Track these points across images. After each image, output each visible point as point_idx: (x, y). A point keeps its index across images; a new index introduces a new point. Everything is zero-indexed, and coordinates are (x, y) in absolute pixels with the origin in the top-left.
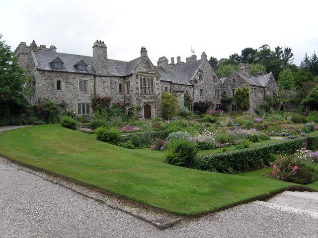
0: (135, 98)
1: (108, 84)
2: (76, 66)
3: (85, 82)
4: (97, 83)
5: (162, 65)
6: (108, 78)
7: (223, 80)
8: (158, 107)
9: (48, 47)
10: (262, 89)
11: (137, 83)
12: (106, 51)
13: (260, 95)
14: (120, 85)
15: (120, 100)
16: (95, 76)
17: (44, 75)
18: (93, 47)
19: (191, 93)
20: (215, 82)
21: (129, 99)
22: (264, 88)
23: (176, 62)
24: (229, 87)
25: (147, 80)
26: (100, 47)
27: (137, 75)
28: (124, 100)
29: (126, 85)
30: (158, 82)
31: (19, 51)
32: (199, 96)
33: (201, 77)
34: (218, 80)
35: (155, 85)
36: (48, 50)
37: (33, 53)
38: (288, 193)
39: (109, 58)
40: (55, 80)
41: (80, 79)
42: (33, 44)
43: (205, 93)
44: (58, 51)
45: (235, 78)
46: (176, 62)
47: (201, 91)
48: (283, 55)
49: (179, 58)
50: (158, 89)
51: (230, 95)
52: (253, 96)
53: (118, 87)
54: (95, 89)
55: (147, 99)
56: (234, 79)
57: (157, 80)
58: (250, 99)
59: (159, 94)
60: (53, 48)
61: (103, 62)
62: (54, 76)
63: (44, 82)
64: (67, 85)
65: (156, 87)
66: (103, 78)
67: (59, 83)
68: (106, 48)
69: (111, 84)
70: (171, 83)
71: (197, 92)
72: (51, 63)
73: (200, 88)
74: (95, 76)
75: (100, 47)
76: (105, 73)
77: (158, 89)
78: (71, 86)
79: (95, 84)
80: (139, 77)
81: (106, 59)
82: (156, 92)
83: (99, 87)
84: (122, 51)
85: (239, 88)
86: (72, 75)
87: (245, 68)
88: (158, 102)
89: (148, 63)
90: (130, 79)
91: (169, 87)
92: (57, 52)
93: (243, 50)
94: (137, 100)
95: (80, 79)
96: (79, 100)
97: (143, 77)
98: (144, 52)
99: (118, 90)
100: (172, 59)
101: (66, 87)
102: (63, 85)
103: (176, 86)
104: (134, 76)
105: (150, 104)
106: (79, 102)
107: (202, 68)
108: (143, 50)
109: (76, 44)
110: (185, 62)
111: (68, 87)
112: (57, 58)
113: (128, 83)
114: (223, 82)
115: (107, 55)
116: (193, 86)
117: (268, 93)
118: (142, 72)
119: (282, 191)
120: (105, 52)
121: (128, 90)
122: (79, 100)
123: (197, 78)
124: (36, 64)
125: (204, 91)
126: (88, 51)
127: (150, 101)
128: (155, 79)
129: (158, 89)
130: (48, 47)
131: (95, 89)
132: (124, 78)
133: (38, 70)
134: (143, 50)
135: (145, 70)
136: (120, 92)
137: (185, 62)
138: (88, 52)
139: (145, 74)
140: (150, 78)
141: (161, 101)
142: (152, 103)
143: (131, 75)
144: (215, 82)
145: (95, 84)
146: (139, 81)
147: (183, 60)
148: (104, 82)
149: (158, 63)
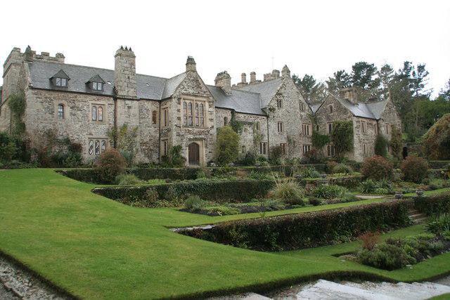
0: (175, 133)
1: (135, 111)
2: (88, 84)
3: (101, 106)
4: (118, 110)
5: (222, 84)
6: (135, 102)
7: (314, 109)
8: (209, 146)
9: (53, 55)
10: (375, 123)
11: (179, 111)
12: (134, 61)
13: (371, 132)
14: (154, 113)
15: (153, 134)
16: (115, 99)
17: (40, 96)
18: (116, 56)
19: (263, 126)
20: (302, 110)
21: (166, 135)
22: (377, 121)
23: (248, 80)
24: (324, 118)
25: (194, 106)
26: (125, 55)
27: (179, 99)
28: (160, 135)
29: (163, 112)
30: (211, 109)
31: (10, 62)
32: (277, 132)
33: (280, 103)
34: (307, 108)
35: (208, 114)
36: (54, 59)
37: (26, 64)
38: (323, 284)
39: (138, 71)
40: (56, 103)
41: (94, 102)
42: (29, 52)
43: (285, 128)
44: (67, 61)
45: (332, 105)
46: (248, 80)
47: (280, 125)
48: (414, 73)
49: (253, 74)
50: (213, 120)
51: (325, 130)
52: (360, 133)
53: (151, 116)
54: (115, 118)
55: (193, 134)
56: (331, 107)
57: (210, 106)
58: (355, 137)
59: (213, 127)
60: (60, 56)
61: (129, 78)
62: (54, 98)
63: (39, 106)
64: (73, 112)
65: (208, 116)
66: (127, 102)
67: (62, 106)
68: (134, 57)
69: (141, 111)
70: (233, 111)
71: (273, 126)
72: (51, 79)
73: (278, 120)
74: (115, 99)
75: (125, 55)
76: (131, 93)
77: (211, 120)
78: (79, 112)
79: (115, 111)
80: (182, 101)
81: (134, 73)
82: (209, 124)
83: (121, 114)
84: (159, 62)
85: (338, 118)
86: (81, 96)
87: (349, 91)
88: (211, 139)
89: (197, 81)
90: (169, 103)
91: (229, 118)
92: (66, 62)
93: (354, 65)
94: (178, 135)
95: (94, 102)
96: (91, 134)
97: (188, 102)
98: (192, 64)
99: (151, 121)
100: (244, 75)
101: (71, 114)
102: (68, 110)
103: (240, 115)
104: (174, 101)
105: (199, 143)
106: (91, 137)
107: (283, 91)
108: (190, 62)
109: (90, 52)
110: (262, 81)
111: (74, 115)
112: (59, 72)
113: (166, 110)
114: (314, 111)
115: (135, 68)
116: (268, 117)
117: (383, 129)
118: (187, 95)
119: (314, 278)
120: (133, 64)
121: (165, 119)
122: (91, 134)
123: (274, 104)
124: (29, 80)
125: (285, 124)
126: (107, 62)
127: (198, 137)
128: (207, 104)
129: (211, 120)
130: (53, 55)
131: (115, 118)
132: (160, 102)
133: (32, 88)
134: (190, 62)
135: (191, 91)
136: (155, 122)
137: (262, 81)
138: (108, 63)
139: (191, 98)
140: (199, 103)
141: (215, 138)
142: (201, 139)
143: (170, 98)
144: (302, 110)
145: (115, 111)
146: (181, 107)
147: (260, 77)
148: (129, 107)
149: (216, 81)
